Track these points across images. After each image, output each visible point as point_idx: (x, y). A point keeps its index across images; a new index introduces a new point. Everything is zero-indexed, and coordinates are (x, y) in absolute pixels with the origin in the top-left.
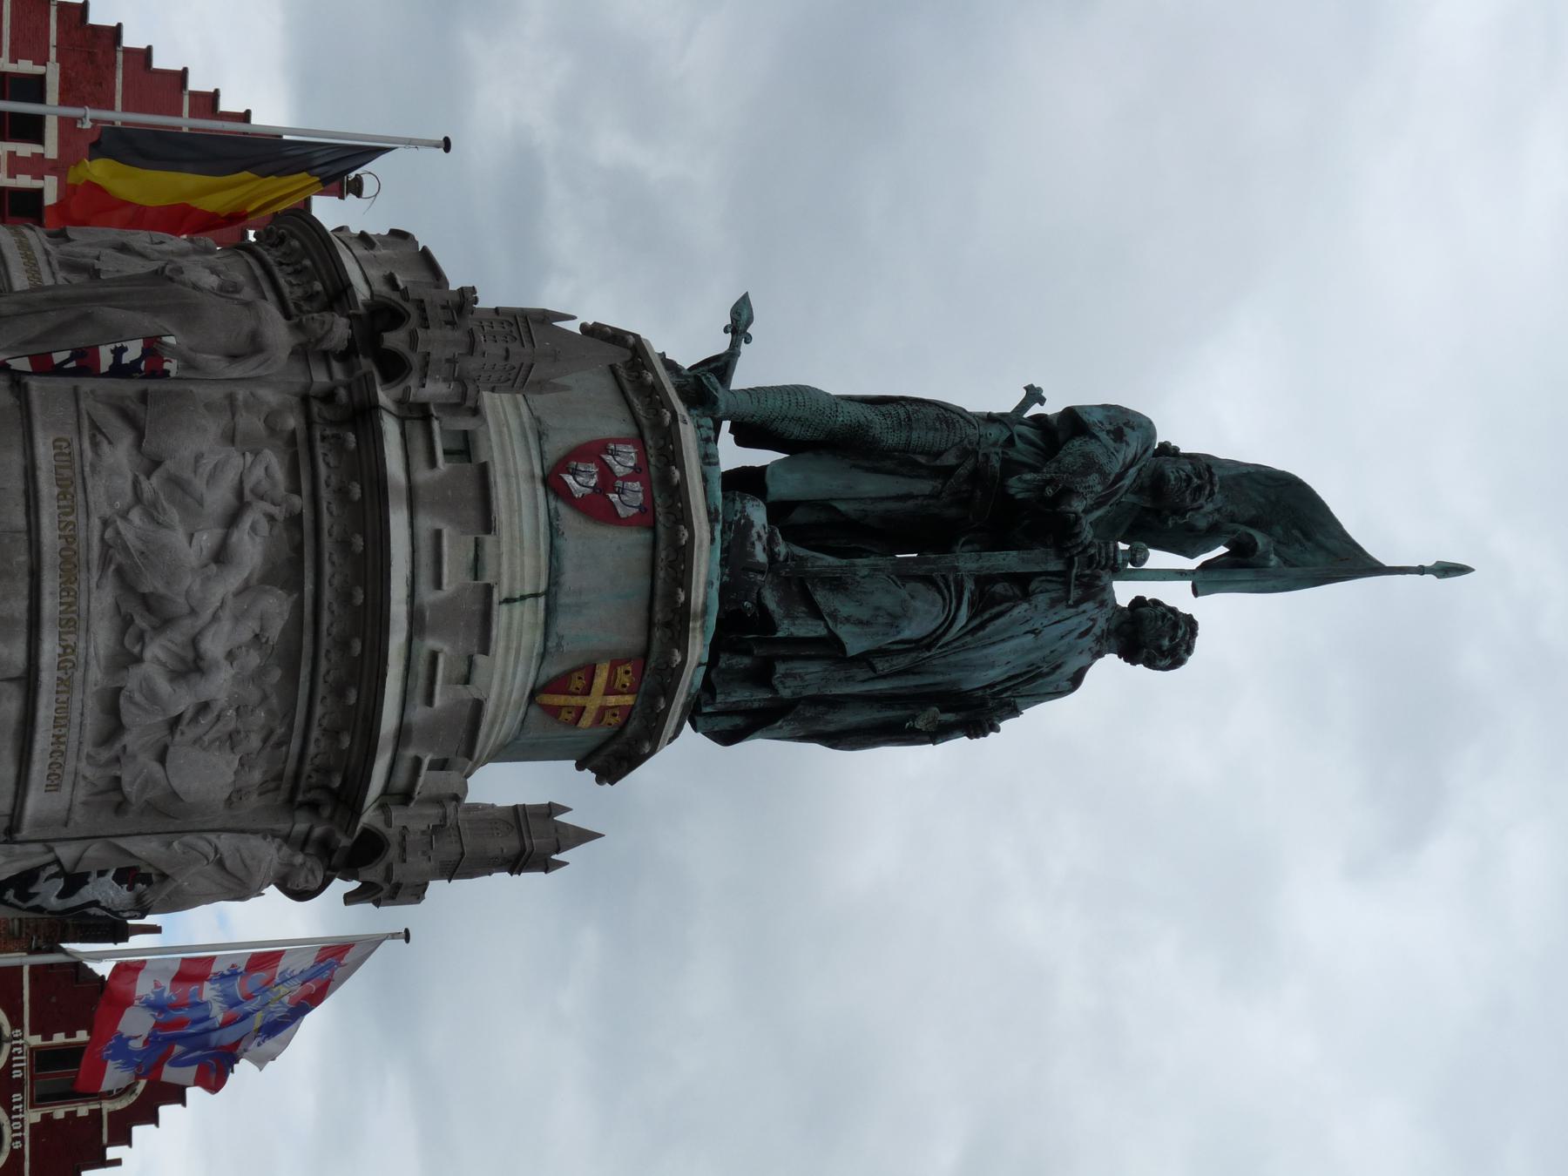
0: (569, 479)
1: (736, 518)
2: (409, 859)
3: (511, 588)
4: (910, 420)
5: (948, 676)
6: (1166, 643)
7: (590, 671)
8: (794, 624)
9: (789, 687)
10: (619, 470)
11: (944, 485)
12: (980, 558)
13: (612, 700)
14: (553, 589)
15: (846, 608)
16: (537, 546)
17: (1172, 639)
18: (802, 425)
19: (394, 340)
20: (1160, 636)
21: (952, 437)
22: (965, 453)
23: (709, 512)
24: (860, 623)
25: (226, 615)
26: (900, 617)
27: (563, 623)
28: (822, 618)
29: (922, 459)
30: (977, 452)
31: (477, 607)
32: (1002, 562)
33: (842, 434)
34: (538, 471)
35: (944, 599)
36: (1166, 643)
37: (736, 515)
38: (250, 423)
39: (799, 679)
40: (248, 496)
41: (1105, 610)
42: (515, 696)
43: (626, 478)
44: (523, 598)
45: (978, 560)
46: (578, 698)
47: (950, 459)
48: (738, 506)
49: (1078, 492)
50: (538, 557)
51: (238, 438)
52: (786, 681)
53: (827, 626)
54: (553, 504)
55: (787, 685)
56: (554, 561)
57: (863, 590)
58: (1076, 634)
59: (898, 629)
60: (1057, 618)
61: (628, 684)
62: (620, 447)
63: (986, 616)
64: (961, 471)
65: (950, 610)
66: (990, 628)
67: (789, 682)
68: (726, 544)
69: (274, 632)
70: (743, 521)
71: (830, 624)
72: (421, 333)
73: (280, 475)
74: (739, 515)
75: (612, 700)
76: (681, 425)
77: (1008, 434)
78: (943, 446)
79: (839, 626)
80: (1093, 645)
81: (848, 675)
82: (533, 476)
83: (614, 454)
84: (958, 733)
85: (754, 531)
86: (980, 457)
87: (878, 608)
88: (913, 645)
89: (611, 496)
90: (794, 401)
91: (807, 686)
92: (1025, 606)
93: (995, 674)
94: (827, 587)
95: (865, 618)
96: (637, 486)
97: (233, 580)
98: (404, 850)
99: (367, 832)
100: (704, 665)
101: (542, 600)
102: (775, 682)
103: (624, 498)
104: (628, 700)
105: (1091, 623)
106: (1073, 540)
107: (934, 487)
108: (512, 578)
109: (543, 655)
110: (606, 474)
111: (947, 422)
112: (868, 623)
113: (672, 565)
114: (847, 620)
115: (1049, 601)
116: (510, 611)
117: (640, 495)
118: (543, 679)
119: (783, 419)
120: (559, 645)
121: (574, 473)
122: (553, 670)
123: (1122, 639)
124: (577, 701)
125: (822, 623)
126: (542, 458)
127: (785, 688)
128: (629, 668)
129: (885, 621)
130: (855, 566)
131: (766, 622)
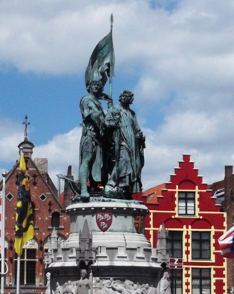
0: (104, 228)
2: (167, 259)
3: (123, 240)
4: (87, 152)
6: (129, 98)
10: (103, 218)
11: (98, 145)
14: (122, 231)
15: (123, 172)
16: (116, 234)
19: (87, 263)
22: (93, 140)
24: (127, 169)
25: (129, 290)
27: (128, 229)
29: (94, 150)
31: (129, 251)
34: (102, 232)
35: (122, 149)
36: (129, 98)
38: (98, 285)
40: (110, 286)
41: (122, 110)
42: (139, 237)
43: (104, 217)
44: (124, 237)
47: (94, 143)
48: (107, 193)
50: (118, 234)
51: (100, 287)
54: (108, 230)
58: (126, 116)
60: (124, 121)
62: (98, 217)
63: (123, 138)
64: (96, 141)
66: (126, 137)
69: (132, 283)
72: (86, 259)
73: (108, 281)
76: (94, 206)
77: (89, 130)
78: (92, 145)
82: (104, 234)
83: (99, 219)
84: (144, 143)
85: (111, 190)
86: (94, 137)
87: (124, 165)
89: (107, 220)
90: (84, 176)
92: (122, 129)
93: (133, 134)
96: (105, 215)
97: (124, 290)
98: (165, 260)
99: (161, 266)
101: (124, 233)
103: (107, 218)
105: (124, 114)
108: (121, 240)
109: (133, 232)
110: (103, 221)
114: (126, 171)
116: (127, 240)
117: (107, 215)
120: (131, 230)
121: (103, 226)
125: (127, 176)
126: (99, 231)
131: (125, 188)
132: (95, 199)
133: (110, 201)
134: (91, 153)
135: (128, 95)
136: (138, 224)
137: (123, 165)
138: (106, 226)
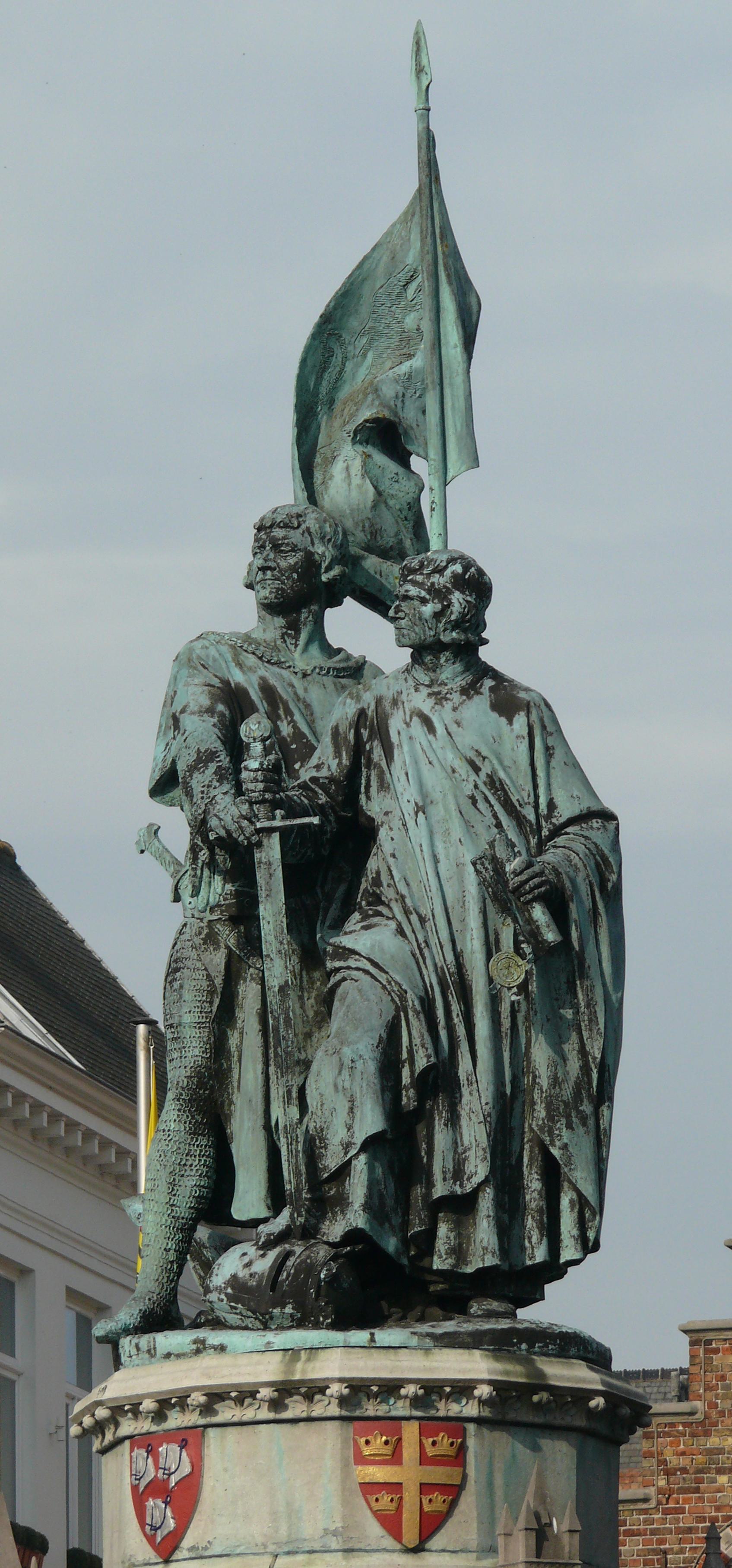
1: (225, 1299)
5: (474, 930)
6: (428, 610)
7: (369, 1488)
8: (352, 1203)
9: (476, 1166)
10: (151, 1474)
12: (268, 956)
13: (410, 1451)
14: (271, 1548)
17: (424, 601)
18: (182, 1176)
20: (420, 619)
21: (189, 963)
22: (211, 939)
23: (198, 1352)
26: (340, 1059)
28: (349, 1162)
30: (210, 921)
32: (271, 926)
33: (193, 1117)
35: (344, 979)
37: (222, 1300)
39: (467, 1154)
45: (271, 959)
46: (406, 1496)
49: (205, 811)
52: (468, 1172)
53: (358, 1154)
55: (473, 1171)
56: (238, 1551)
57: (319, 1107)
59: (356, 1058)
61: (384, 1438)
65: (357, 969)
67: (469, 1168)
68: (250, 1314)
70: (229, 1291)
71: (353, 1152)
74: (223, 1296)
75: (410, 1451)
79: (354, 1140)
80: (448, 706)
81: (466, 1082)
85: (243, 1274)
87: (336, 1086)
88: (402, 1014)
91: (476, 1141)
94: (323, 1151)
95: (347, 1105)
100: (372, 1335)
102: (468, 1188)
104: (410, 1432)
105: (416, 719)
106: (234, 835)
107: (252, 979)
111: (177, 970)
112: (352, 1101)
113: (240, 1401)
114: (349, 1128)
115: (383, 793)
118: (389, 1542)
119: (172, 1205)
120: (335, 1533)
122: (374, 1530)
123: (442, 661)
124: (411, 1496)
125: (353, 1162)
127: (476, 1174)
128: (363, 1440)
129: (347, 1077)
130: (286, 1126)
132: (137, 1347)
133: (200, 1348)
134: (195, 1033)
135: (413, 591)
136: (395, 1488)
137: (331, 1088)
138: (171, 1524)
